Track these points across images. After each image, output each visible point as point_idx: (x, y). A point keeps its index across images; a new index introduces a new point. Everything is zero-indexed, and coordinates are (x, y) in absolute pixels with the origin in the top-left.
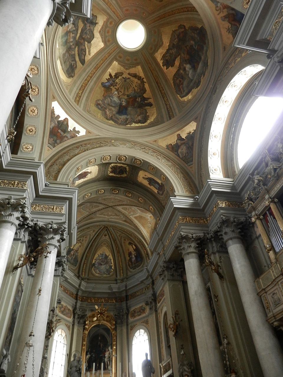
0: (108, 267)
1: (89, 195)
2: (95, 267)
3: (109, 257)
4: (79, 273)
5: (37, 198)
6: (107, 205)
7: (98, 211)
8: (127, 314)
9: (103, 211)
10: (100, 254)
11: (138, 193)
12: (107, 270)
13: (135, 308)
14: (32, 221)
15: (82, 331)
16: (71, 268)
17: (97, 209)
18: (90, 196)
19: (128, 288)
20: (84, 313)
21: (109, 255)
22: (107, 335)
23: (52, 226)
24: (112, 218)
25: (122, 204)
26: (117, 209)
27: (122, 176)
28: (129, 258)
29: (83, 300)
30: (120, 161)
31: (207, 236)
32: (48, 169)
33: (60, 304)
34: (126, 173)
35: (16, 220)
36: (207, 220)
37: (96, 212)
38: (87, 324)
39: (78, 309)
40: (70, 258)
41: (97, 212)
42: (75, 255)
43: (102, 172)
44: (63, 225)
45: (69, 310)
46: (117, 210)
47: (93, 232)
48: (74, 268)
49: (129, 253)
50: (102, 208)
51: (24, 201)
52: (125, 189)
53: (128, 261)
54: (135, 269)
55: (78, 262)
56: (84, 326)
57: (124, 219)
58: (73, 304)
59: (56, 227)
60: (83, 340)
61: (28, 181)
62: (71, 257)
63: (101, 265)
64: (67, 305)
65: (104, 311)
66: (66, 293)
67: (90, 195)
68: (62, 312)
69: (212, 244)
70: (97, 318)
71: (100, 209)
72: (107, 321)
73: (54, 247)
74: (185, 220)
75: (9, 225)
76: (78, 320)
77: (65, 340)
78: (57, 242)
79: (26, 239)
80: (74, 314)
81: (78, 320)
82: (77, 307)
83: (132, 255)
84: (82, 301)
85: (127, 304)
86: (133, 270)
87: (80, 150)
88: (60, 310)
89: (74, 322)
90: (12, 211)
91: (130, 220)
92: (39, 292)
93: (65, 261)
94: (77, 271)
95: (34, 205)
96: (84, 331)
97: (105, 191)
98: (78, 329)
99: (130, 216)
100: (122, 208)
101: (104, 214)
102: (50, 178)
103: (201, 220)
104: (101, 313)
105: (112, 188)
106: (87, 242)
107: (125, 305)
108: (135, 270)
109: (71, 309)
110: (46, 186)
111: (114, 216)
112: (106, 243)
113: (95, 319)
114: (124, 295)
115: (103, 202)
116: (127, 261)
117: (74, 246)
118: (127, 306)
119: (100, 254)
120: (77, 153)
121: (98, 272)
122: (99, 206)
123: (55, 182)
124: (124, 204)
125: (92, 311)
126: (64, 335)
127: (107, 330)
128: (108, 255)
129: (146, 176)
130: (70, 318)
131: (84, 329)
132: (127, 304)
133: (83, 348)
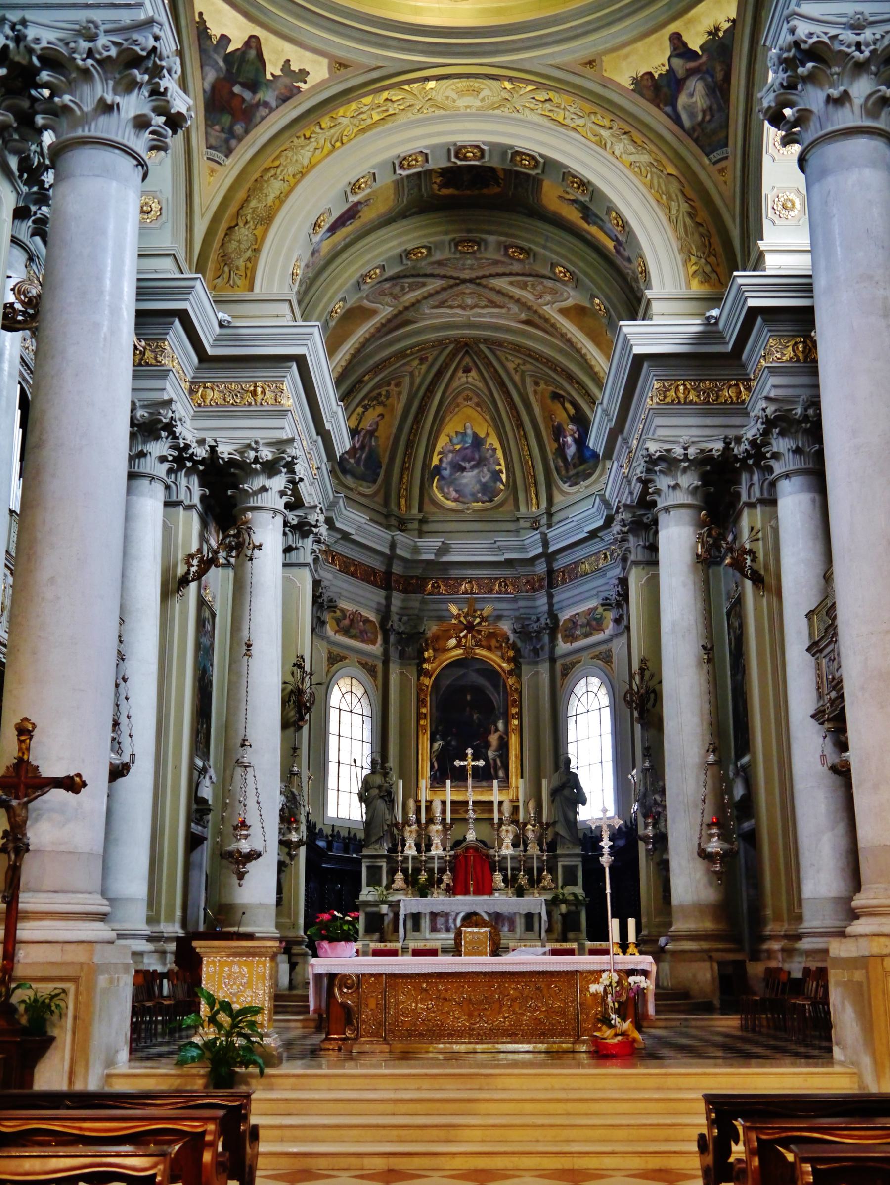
0: (486, 477)
1: (375, 274)
2: (442, 478)
3: (489, 441)
4: (386, 503)
5: (204, 365)
6: (452, 277)
7: (425, 298)
9: (444, 296)
10: (454, 435)
11: (551, 250)
12: (485, 488)
14: (201, 442)
15: (414, 679)
16: (360, 493)
17: (417, 293)
18: (381, 275)
19: (551, 550)
21: (487, 435)
22: (492, 689)
23: (258, 454)
24: (481, 315)
25: (507, 271)
26: (491, 286)
27: (485, 191)
28: (556, 445)
30: (461, 160)
31: (736, 451)
32: (223, 245)
34: (498, 185)
35: (159, 464)
36: (748, 389)
37: (418, 302)
38: (429, 658)
40: (352, 461)
41: (424, 302)
42: (367, 449)
43: (409, 190)
44: (288, 450)
45: (367, 621)
46: (492, 289)
47: (421, 363)
48: (368, 491)
49: (553, 426)
50: (438, 289)
51: (170, 414)
52: (503, 239)
53: (554, 454)
54: (576, 484)
55: (381, 467)
56: (419, 665)
57: (523, 315)
58: (378, 603)
59: (270, 457)
60: (420, 702)
61: (168, 337)
62: (354, 457)
63: (463, 469)
64: (357, 608)
65: (478, 620)
66: (352, 575)
67: (378, 271)
68: (346, 632)
69: (752, 474)
71: (432, 291)
72: (489, 649)
73: (270, 514)
74: (672, 393)
75: (145, 482)
76: (399, 648)
77: (365, 702)
78: (278, 496)
79: (196, 500)
81: (399, 648)
82: (394, 609)
83: (565, 437)
84: (405, 591)
85: (550, 597)
86: (570, 486)
87: (316, 149)
89: (386, 653)
90: (145, 442)
91: (547, 320)
92: (248, 650)
93: (317, 521)
94: (380, 499)
95: (199, 387)
96: (422, 678)
97: (429, 249)
98: (401, 673)
99: (545, 308)
100: (511, 283)
101: (450, 303)
102: (231, 282)
103: (730, 386)
104: (470, 627)
105: (453, 239)
106: (404, 398)
107: (545, 600)
108: (575, 489)
109: (372, 617)
110: (221, 325)
111: (486, 307)
112: (470, 394)
113: (453, 642)
114: (541, 568)
115: (437, 272)
116: (550, 456)
117: (361, 418)
118: (551, 604)
119: (457, 433)
120: (306, 162)
121: (454, 494)
122: (424, 285)
123: (249, 296)
124: (514, 272)
125: (440, 619)
126: (359, 691)
127: (492, 674)
128: (482, 435)
129: (568, 193)
130: (374, 642)
131: (421, 672)
132: (550, 597)
133: (422, 722)
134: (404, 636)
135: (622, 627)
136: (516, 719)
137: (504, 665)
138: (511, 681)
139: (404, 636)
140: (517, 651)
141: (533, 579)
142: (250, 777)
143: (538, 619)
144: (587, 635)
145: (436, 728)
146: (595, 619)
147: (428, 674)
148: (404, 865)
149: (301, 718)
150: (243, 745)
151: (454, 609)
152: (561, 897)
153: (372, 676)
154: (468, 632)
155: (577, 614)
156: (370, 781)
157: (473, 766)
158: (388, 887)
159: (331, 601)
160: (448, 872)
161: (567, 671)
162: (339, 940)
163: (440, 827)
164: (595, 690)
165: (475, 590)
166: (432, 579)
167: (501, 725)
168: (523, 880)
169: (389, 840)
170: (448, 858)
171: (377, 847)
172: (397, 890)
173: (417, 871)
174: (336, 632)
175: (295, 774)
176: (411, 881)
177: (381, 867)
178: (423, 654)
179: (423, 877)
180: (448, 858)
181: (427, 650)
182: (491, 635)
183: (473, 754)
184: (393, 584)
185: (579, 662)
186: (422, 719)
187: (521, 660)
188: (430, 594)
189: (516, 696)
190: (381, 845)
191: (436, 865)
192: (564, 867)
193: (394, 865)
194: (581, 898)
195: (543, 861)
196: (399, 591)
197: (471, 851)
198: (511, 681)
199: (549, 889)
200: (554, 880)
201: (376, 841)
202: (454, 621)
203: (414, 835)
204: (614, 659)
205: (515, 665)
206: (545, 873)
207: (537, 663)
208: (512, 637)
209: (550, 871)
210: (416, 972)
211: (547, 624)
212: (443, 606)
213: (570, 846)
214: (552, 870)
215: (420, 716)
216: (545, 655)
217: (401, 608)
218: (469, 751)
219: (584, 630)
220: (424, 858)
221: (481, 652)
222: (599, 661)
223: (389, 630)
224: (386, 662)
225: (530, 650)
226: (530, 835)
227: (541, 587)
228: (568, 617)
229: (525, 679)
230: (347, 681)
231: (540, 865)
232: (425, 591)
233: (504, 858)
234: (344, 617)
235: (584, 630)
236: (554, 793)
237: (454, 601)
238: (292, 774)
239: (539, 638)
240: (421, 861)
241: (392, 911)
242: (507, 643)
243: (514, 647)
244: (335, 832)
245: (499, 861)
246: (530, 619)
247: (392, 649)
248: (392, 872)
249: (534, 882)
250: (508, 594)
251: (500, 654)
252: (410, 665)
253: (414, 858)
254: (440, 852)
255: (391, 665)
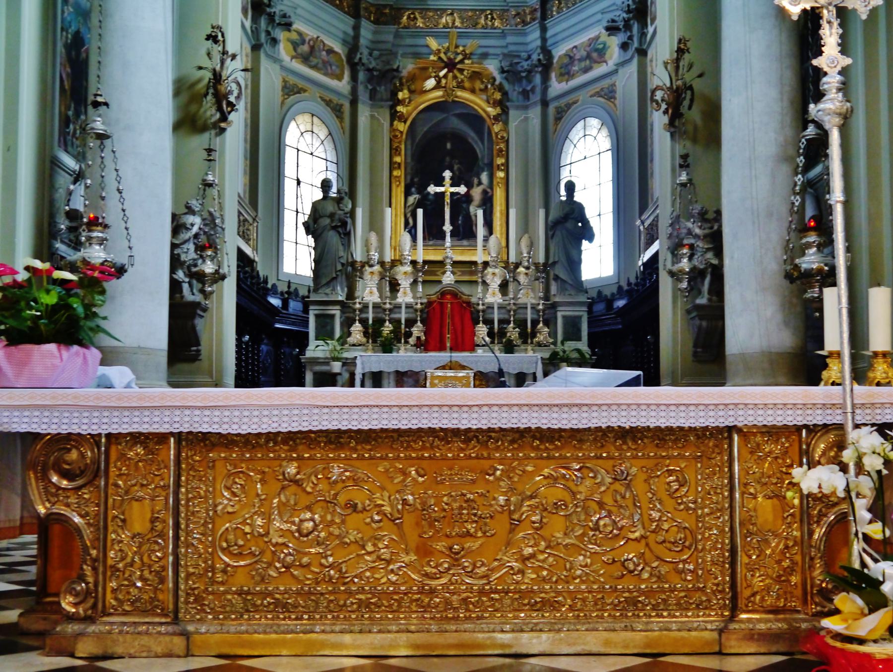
8: (543, 65)
13: (571, 46)
20: (388, 63)
22: (476, 138)
29: (382, 19)
33: (289, 31)
39: (365, 52)
45: (330, 51)
56: (393, 109)
58: (345, 33)
60: (394, 151)
64: (319, 34)
65: (460, 57)
68: (305, 59)
70: (439, 82)
72: (473, 91)
76: (370, 87)
77: (329, 146)
80: (354, 67)
81: (370, 87)
82: (363, 42)
84: (376, 22)
85: (544, 29)
88: (294, 53)
89: (354, 91)
96: (395, 123)
98: (372, 117)
104: (451, 65)
107: (537, 34)
109: (338, 48)
113: (431, 83)
118: (544, 39)
125: (417, 56)
126: (322, 132)
127: (475, 120)
130: (339, 78)
131: (394, 116)
132: (544, 29)
133: (395, 173)
134: (375, 73)
135: (631, 52)
136: (502, 170)
137: (489, 109)
138: (496, 128)
139: (375, 73)
140: (505, 94)
141: (524, 11)
142: (107, 153)
143: (529, 57)
144: (586, 70)
145: (412, 179)
146: (597, 50)
147: (402, 118)
148: (364, 316)
149: (224, 118)
150: (96, 105)
151: (433, 44)
152: (561, 354)
153: (337, 117)
154: (449, 71)
155: (575, 47)
156: (319, 208)
157: (452, 194)
158: (343, 341)
159: (284, 16)
160: (419, 324)
161: (560, 114)
162: (35, 337)
163: (408, 268)
164: (594, 132)
165: (458, 23)
166: (408, 9)
167: (484, 177)
168: (513, 332)
169: (345, 284)
170: (419, 306)
171: (328, 291)
172: (354, 345)
173: (379, 322)
174: (293, 58)
175: (210, 185)
176: (372, 333)
177: (332, 317)
178: (396, 94)
179: (387, 328)
180: (419, 306)
181: (401, 90)
182: (476, 76)
183: (451, 179)
184: (362, 12)
185: (575, 103)
186: (395, 169)
187: (508, 104)
188: (405, 27)
189: (502, 146)
190: (334, 290)
191: (403, 316)
192: (564, 317)
193: (351, 315)
194: (588, 356)
195: (539, 311)
196: (369, 19)
197: (448, 297)
198: (496, 128)
199: (545, 346)
200: (553, 334)
201: (328, 284)
202: (432, 58)
203: (376, 278)
204: (619, 95)
205: (502, 109)
206: (541, 325)
207: (526, 108)
208: (499, 79)
209: (547, 323)
210: (264, 429)
211: (539, 60)
212: (420, 41)
213: (573, 292)
214: (550, 322)
215: (393, 166)
216: (536, 97)
217: (373, 42)
218: (447, 174)
219: (583, 64)
220: (388, 306)
221: (464, 95)
222: (601, 99)
223: (357, 64)
224: (354, 103)
225: (519, 93)
226: (522, 279)
227: (533, 19)
228: (563, 52)
229: (513, 125)
230: (307, 117)
231: (535, 316)
232: (400, 23)
233: (490, 307)
234: (303, 42)
235: (583, 64)
236: (552, 228)
237: (436, 36)
238: (208, 185)
239: (529, 78)
240: (385, 310)
241: (347, 370)
242: (493, 84)
243: (500, 88)
244: (292, 289)
245: (483, 311)
246: (519, 56)
247: (361, 88)
248: (348, 323)
249: (527, 336)
250: (495, 29)
251: (484, 97)
252: (382, 107)
253: (376, 306)
254: (409, 299)
255: (361, 107)
